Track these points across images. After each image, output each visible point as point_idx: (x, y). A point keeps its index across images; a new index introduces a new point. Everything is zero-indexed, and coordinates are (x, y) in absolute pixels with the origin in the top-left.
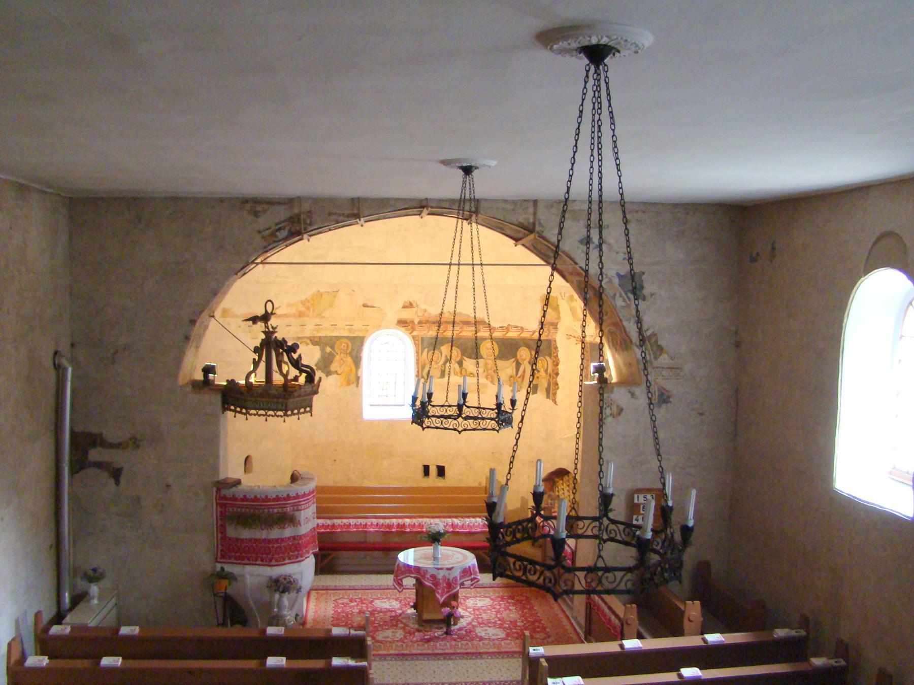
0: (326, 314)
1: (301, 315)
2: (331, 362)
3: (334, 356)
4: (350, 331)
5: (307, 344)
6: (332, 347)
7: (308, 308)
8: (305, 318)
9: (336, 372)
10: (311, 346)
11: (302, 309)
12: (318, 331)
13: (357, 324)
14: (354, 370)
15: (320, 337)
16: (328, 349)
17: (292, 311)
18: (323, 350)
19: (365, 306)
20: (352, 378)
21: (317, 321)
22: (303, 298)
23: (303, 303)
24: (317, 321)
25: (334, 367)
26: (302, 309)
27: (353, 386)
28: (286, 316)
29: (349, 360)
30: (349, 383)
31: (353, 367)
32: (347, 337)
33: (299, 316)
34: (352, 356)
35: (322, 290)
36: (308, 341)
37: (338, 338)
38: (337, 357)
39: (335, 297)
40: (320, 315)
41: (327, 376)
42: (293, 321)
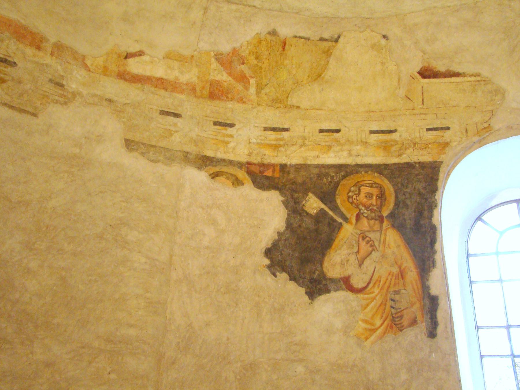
0: (303, 98)
1: (216, 93)
2: (326, 245)
3: (335, 228)
4: (386, 147)
5: (237, 182)
6: (328, 197)
7: (243, 79)
8: (230, 105)
9: (346, 283)
10: (249, 189)
11: (223, 77)
12: (276, 147)
13: (409, 128)
14: (412, 275)
15: (283, 167)
16: (313, 204)
17: (189, 76)
18: (294, 208)
19: (426, 73)
20: (409, 299)
21: (273, 117)
22: (226, 48)
23: (226, 61)
24: (273, 117)
25: (337, 262)
26: (223, 77)
27: (416, 334)
28: (160, 83)
29: (392, 238)
30: (396, 323)
31: (409, 264)
32: (380, 169)
33: (212, 96)
34: (400, 228)
35: (285, 32)
36: (242, 174)
37: (345, 171)
38: (348, 230)
39: (328, 53)
40: (279, 102)
41: (312, 295)
42: (187, 104)
